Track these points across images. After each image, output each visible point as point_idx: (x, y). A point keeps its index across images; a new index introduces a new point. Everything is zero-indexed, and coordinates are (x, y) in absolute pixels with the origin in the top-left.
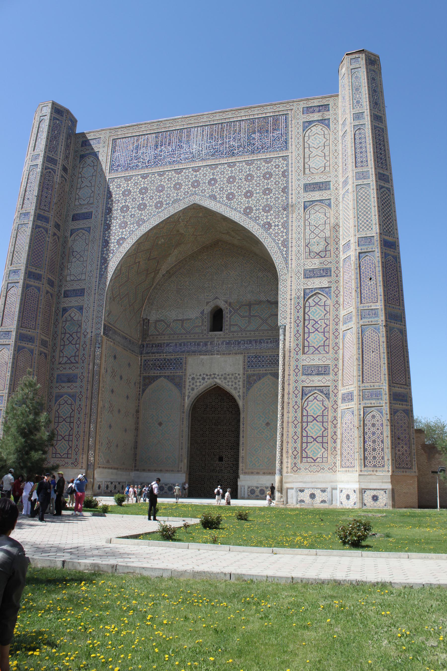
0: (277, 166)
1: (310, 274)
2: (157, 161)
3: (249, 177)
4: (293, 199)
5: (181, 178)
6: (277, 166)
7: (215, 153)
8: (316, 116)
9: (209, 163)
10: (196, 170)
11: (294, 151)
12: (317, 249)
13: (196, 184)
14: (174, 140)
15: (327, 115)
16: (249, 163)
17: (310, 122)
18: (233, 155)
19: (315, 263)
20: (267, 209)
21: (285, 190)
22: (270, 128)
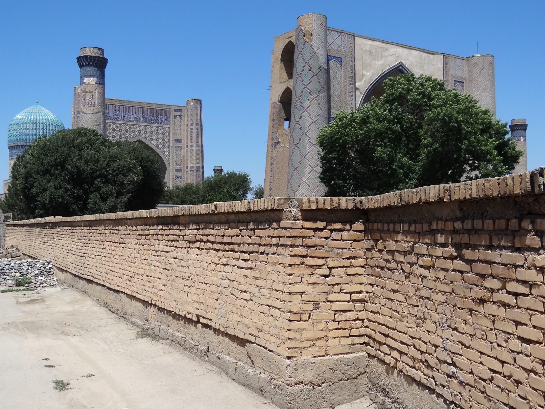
0: (166, 131)
1: (177, 171)
2: (124, 118)
3: (158, 133)
4: (171, 144)
5: (134, 128)
6: (166, 131)
7: (146, 121)
8: (178, 114)
9: (144, 124)
10: (140, 126)
11: (171, 125)
12: (179, 163)
13: (140, 132)
14: (131, 111)
15: (182, 114)
16: (158, 127)
17: (177, 116)
18: (152, 123)
19: (178, 168)
20: (164, 146)
21: (169, 140)
22: (164, 115)
